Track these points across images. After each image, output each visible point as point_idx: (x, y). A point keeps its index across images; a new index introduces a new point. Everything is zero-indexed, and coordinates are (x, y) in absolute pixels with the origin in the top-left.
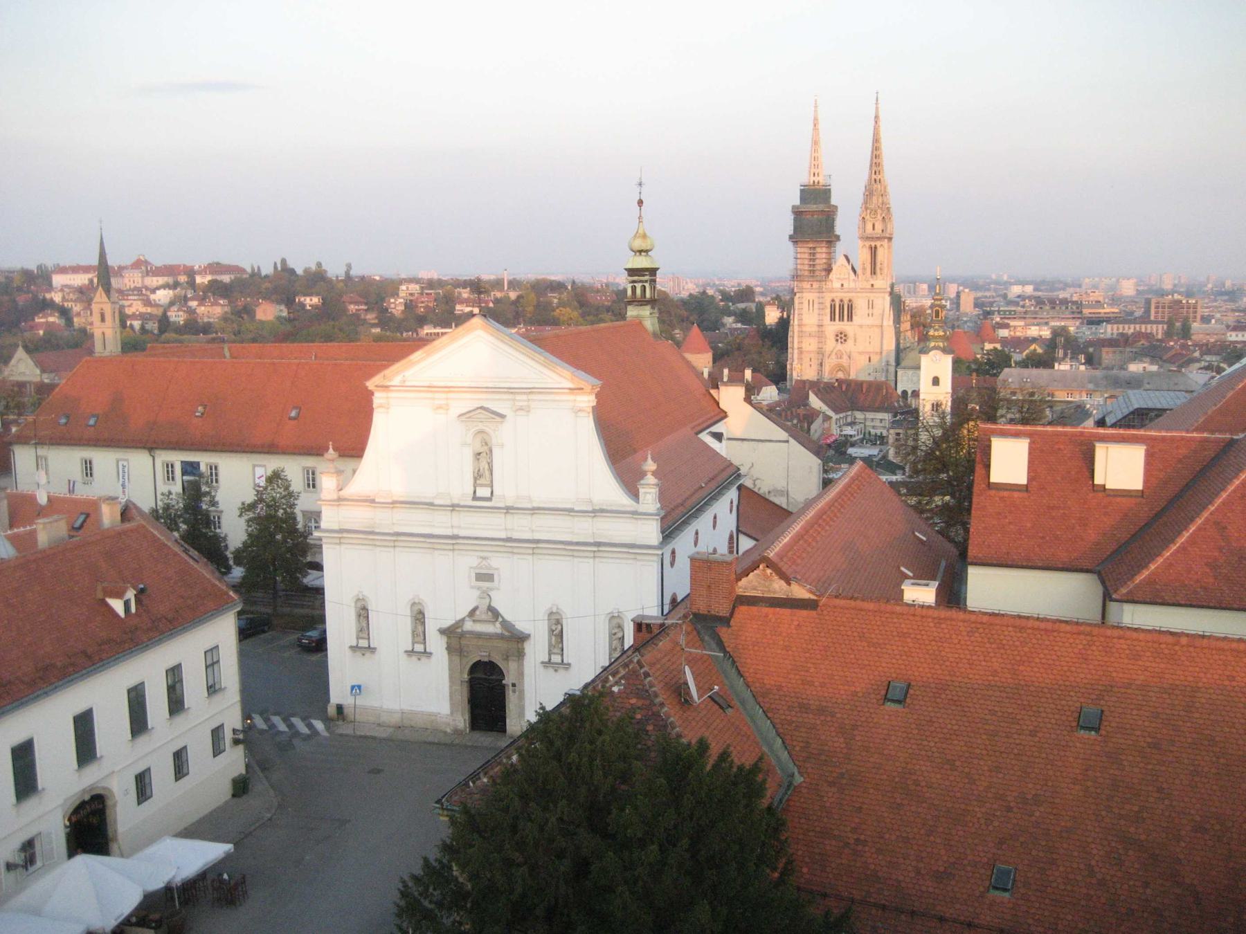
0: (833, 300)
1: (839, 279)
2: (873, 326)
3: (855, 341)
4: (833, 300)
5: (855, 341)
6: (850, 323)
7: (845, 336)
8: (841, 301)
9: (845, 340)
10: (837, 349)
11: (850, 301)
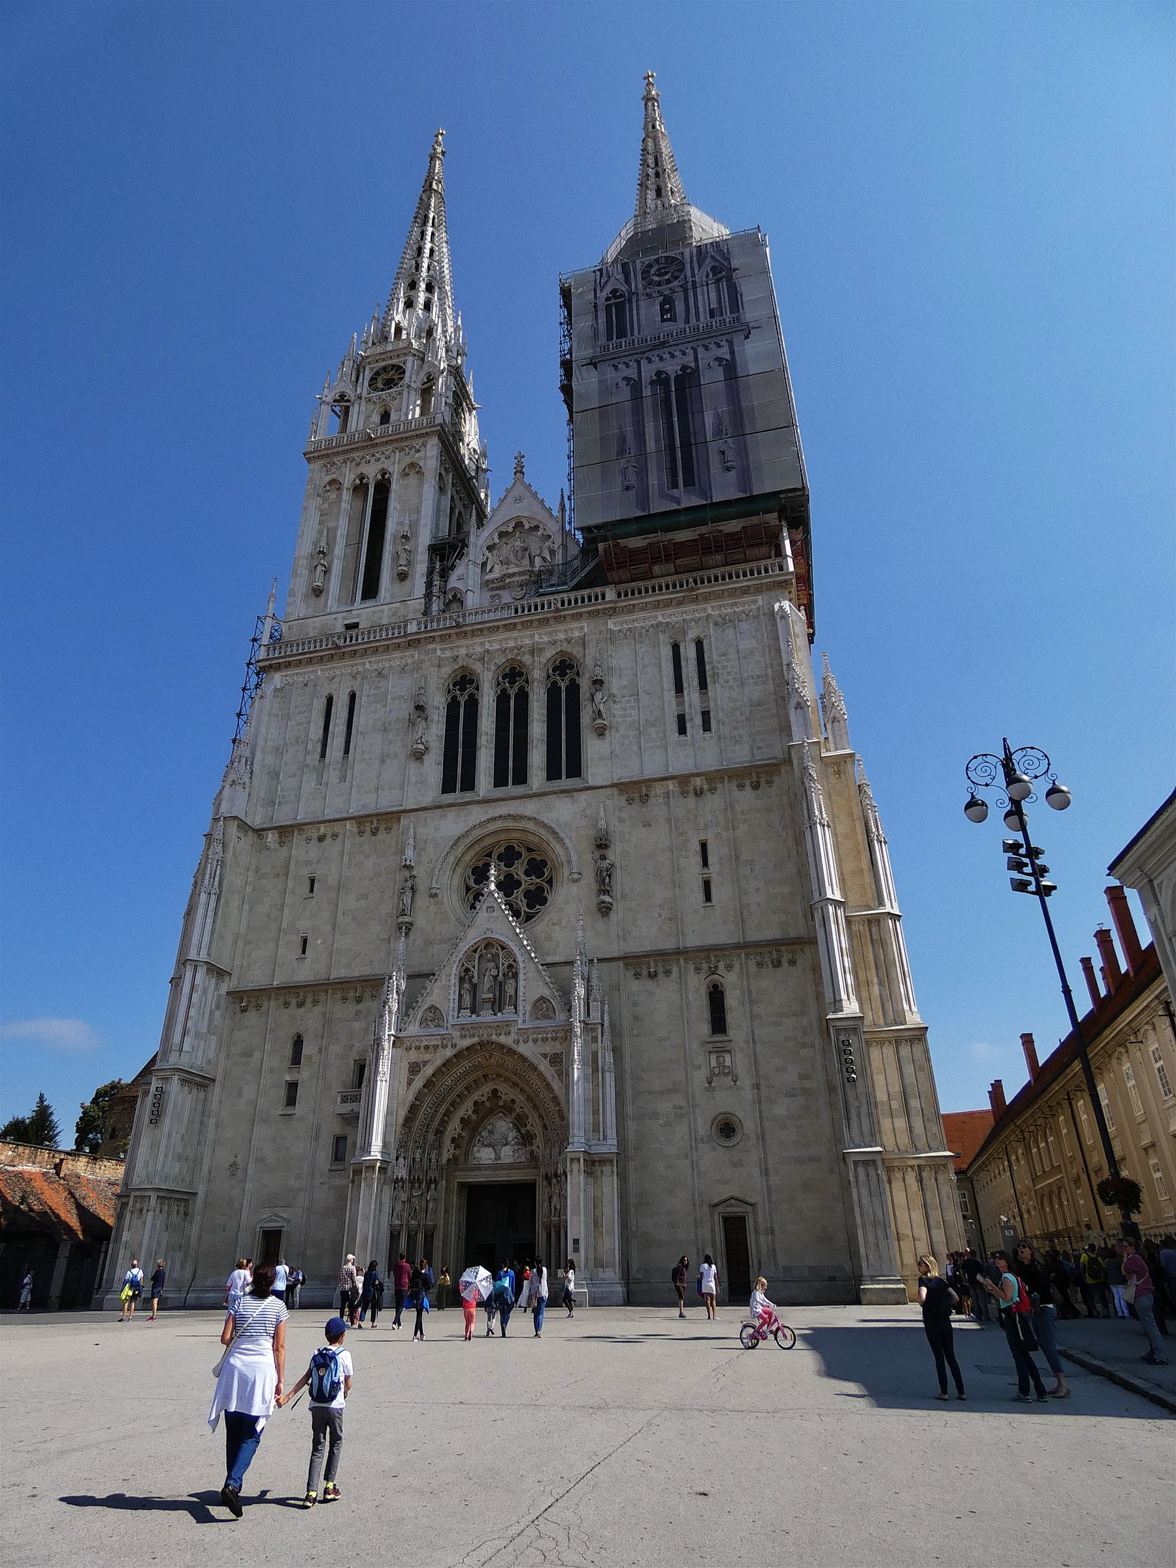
0: (465, 681)
1: (501, 584)
2: (714, 778)
3: (604, 881)
4: (465, 681)
5: (604, 881)
6: (565, 783)
7: (537, 867)
8: (514, 673)
9: (537, 898)
10: (473, 936)
11: (564, 666)
